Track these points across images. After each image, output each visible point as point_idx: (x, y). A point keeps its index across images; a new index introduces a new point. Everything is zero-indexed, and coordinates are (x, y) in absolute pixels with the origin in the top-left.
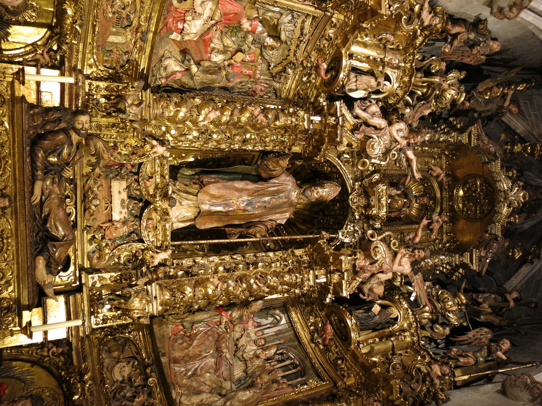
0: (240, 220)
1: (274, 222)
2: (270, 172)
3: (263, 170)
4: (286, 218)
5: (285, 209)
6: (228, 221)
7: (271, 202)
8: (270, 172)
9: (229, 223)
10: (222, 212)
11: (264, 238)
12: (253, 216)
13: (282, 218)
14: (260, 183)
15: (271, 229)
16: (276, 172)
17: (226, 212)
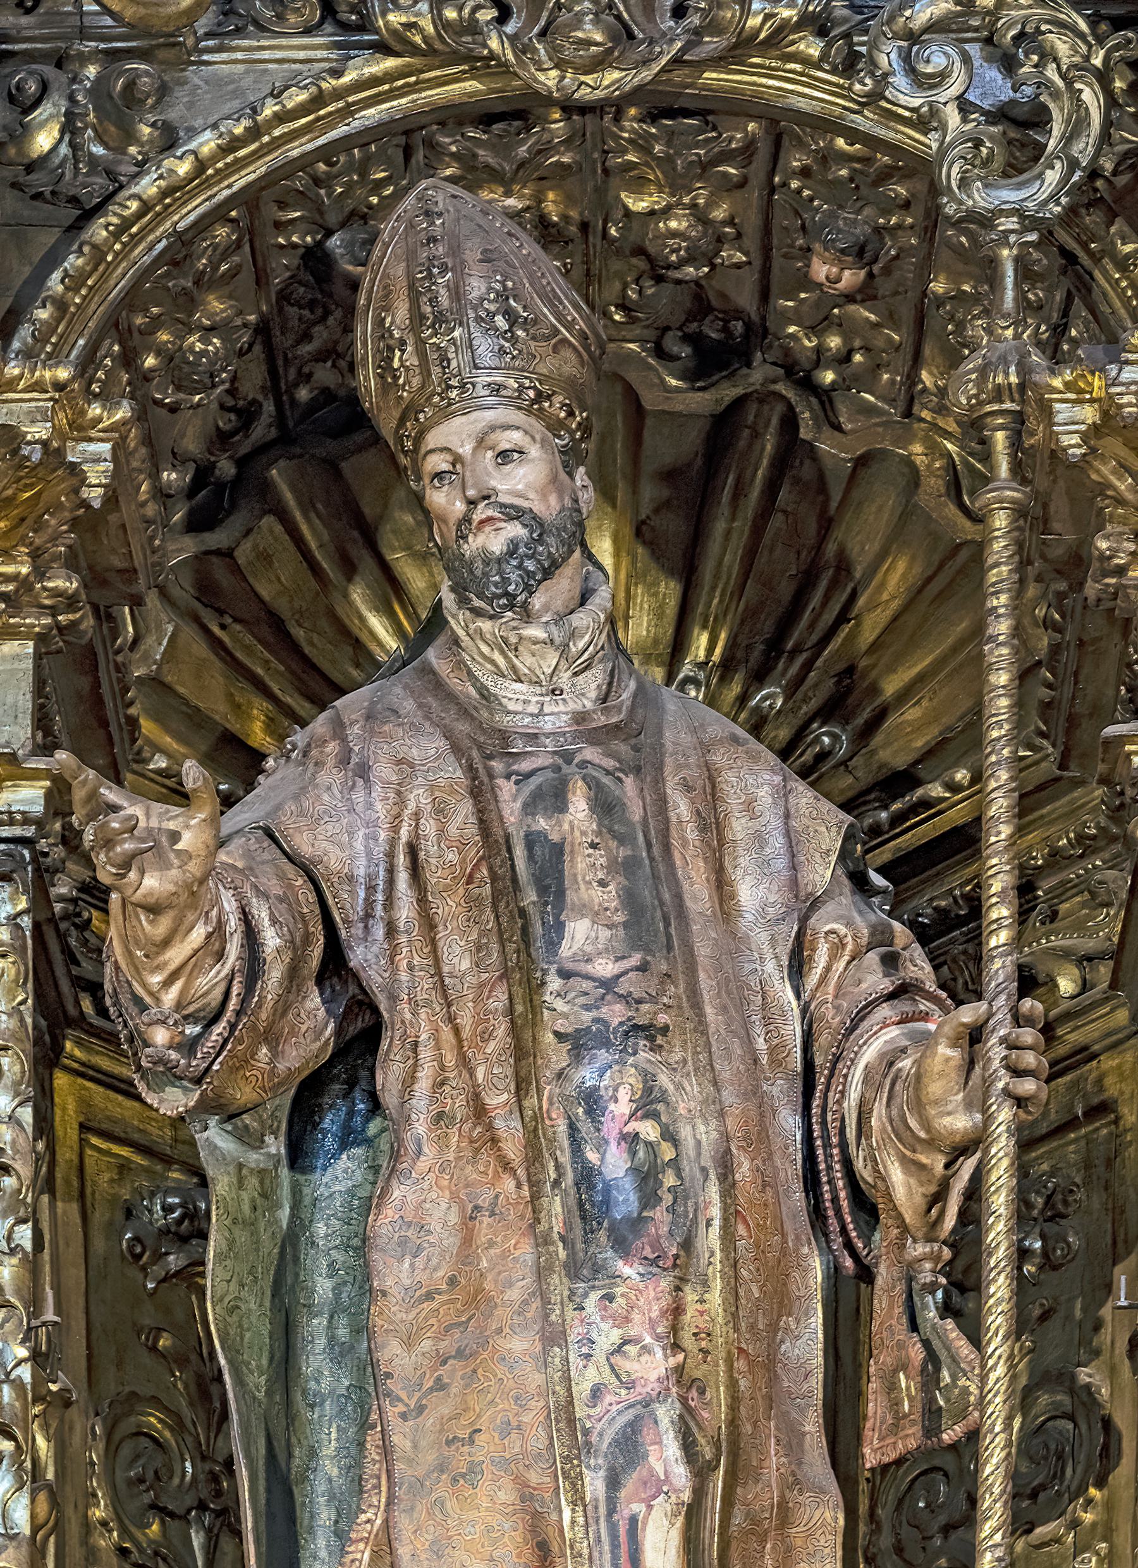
0: (781, 1301)
1: (825, 923)
2: (274, 976)
3: (245, 1061)
4: (783, 794)
5: (681, 807)
6: (793, 1444)
7: (605, 968)
8: (274, 976)
9: (812, 1425)
10: (693, 1513)
11: (996, 1052)
12: (744, 1169)
13: (772, 837)
14: (388, 1077)
15: (891, 961)
16: (261, 913)
17: (701, 1472)
